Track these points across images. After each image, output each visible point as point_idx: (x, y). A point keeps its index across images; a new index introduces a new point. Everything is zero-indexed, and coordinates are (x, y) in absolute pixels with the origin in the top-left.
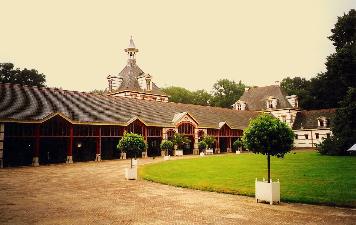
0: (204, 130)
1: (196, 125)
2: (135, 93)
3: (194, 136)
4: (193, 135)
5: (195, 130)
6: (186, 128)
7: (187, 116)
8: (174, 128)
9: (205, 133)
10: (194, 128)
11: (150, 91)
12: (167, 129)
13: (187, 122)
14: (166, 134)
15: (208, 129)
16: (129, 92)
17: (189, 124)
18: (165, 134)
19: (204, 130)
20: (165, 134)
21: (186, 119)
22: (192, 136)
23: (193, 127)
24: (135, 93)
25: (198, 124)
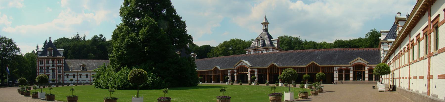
0: (255, 70)
9: (255, 71)
10: (248, 69)
12: (230, 71)
15: (257, 68)
16: (247, 50)
19: (255, 70)
21: (242, 64)
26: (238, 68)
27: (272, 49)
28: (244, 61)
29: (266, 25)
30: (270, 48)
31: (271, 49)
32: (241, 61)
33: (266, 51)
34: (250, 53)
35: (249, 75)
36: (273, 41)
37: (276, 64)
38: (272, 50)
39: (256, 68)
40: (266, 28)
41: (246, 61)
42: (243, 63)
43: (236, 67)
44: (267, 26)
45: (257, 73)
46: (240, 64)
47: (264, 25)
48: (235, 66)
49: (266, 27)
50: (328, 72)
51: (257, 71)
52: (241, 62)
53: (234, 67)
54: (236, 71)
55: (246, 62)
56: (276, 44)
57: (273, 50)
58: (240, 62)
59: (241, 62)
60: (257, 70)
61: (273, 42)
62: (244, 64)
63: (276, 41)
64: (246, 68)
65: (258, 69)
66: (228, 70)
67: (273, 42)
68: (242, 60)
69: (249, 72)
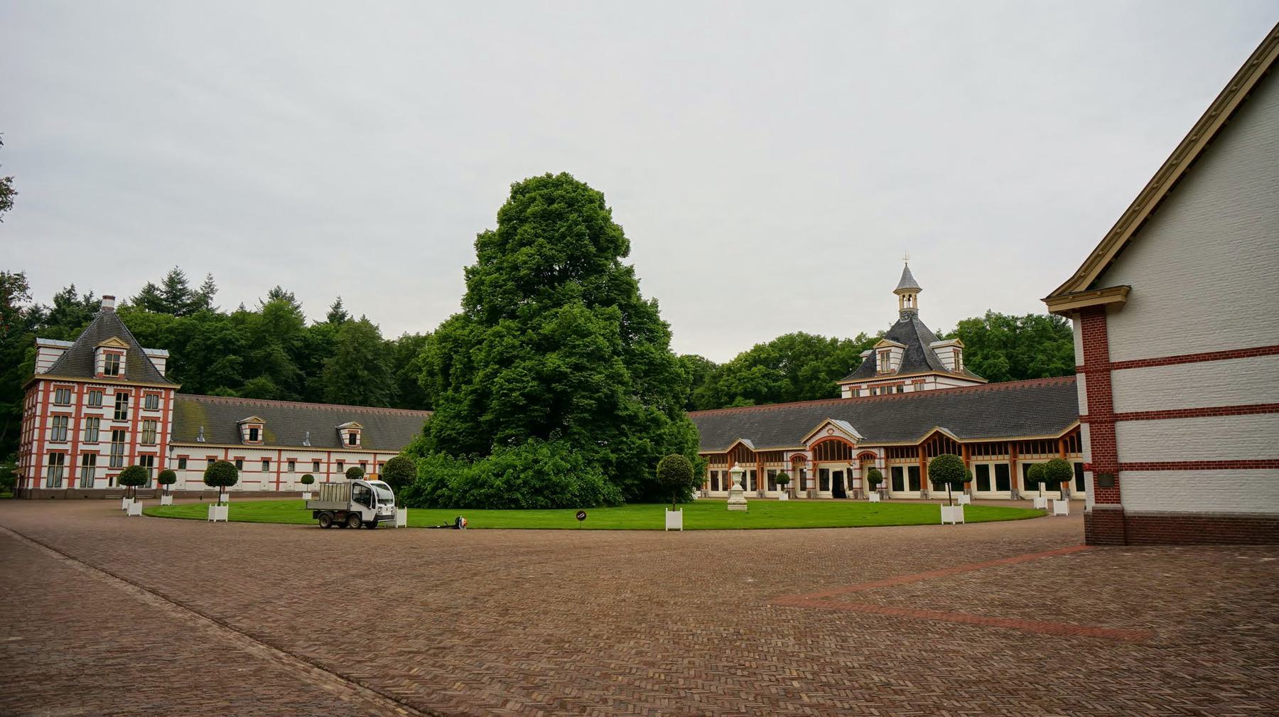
0: (876, 451)
2: (857, 383)
5: (853, 451)
6: (833, 452)
8: (804, 450)
9: (878, 456)
10: (850, 449)
12: (790, 454)
13: (832, 438)
15: (884, 447)
16: (846, 384)
17: (839, 442)
19: (876, 451)
21: (831, 432)
24: (857, 383)
26: (819, 445)
27: (935, 380)
28: (838, 423)
29: (910, 296)
30: (928, 376)
31: (932, 379)
32: (829, 423)
33: (912, 386)
34: (858, 394)
35: (855, 469)
36: (937, 351)
37: (945, 431)
38: (935, 382)
39: (880, 447)
40: (911, 306)
41: (843, 422)
42: (834, 429)
43: (809, 444)
44: (916, 299)
45: (883, 461)
46: (824, 434)
47: (904, 296)
48: (807, 440)
49: (911, 302)
51: (883, 456)
52: (826, 425)
53: (805, 443)
54: (809, 455)
55: (845, 425)
56: (953, 360)
57: (939, 380)
58: (824, 427)
59: (826, 425)
60: (883, 451)
61: (937, 354)
62: (837, 433)
63: (951, 349)
64: (845, 445)
66: (783, 451)
67: (937, 354)
68: (829, 420)
69: (855, 459)
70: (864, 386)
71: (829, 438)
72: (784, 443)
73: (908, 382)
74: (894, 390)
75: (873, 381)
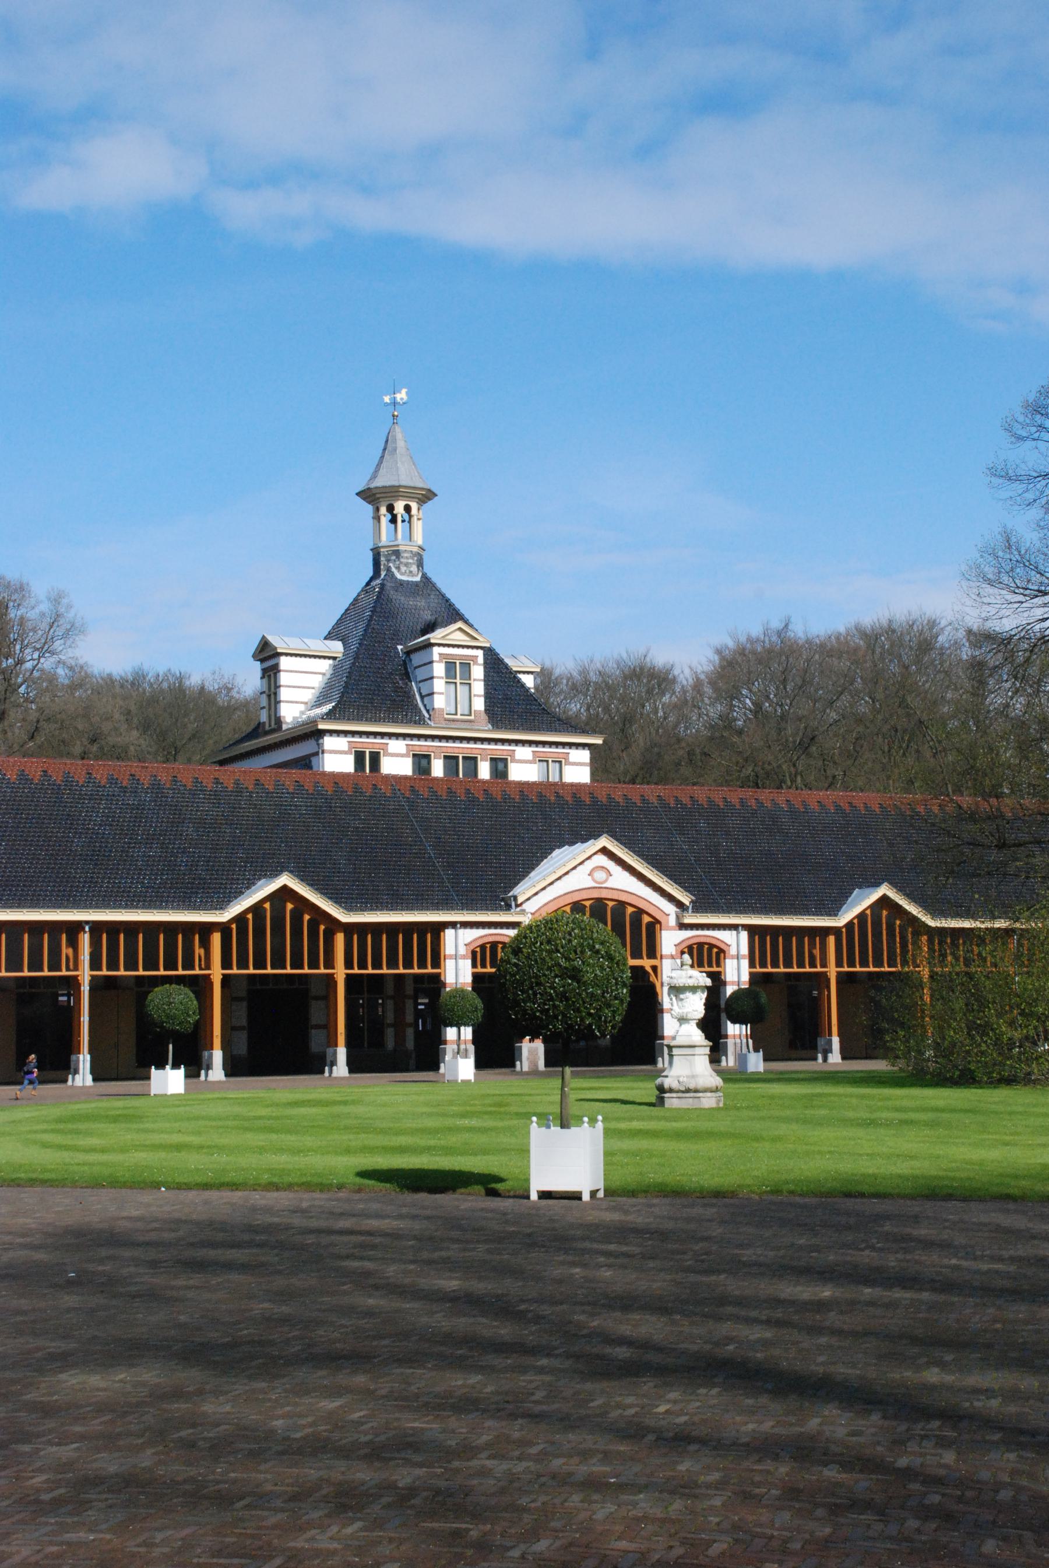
1: (670, 909)
3: (655, 968)
4: (646, 963)
7: (602, 860)
9: (733, 951)
11: (472, 717)
13: (604, 894)
14: (464, 957)
15: (745, 927)
16: (338, 733)
18: (456, 957)
20: (456, 957)
21: (600, 875)
22: (642, 968)
23: (646, 919)
25: (679, 904)
30: (577, 746)
45: (745, 963)
50: (765, 966)
51: (745, 950)
60: (744, 935)
65: (751, 930)
66: (445, 925)
70: (397, 746)
71: (596, 894)
72: (445, 905)
73: (524, 752)
74: (484, 771)
75: (426, 737)
